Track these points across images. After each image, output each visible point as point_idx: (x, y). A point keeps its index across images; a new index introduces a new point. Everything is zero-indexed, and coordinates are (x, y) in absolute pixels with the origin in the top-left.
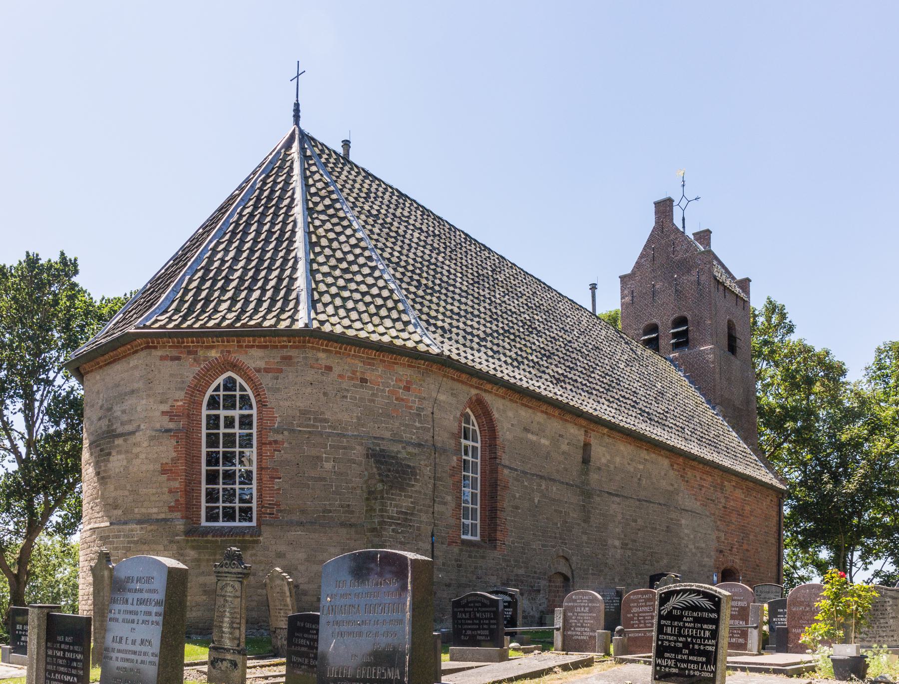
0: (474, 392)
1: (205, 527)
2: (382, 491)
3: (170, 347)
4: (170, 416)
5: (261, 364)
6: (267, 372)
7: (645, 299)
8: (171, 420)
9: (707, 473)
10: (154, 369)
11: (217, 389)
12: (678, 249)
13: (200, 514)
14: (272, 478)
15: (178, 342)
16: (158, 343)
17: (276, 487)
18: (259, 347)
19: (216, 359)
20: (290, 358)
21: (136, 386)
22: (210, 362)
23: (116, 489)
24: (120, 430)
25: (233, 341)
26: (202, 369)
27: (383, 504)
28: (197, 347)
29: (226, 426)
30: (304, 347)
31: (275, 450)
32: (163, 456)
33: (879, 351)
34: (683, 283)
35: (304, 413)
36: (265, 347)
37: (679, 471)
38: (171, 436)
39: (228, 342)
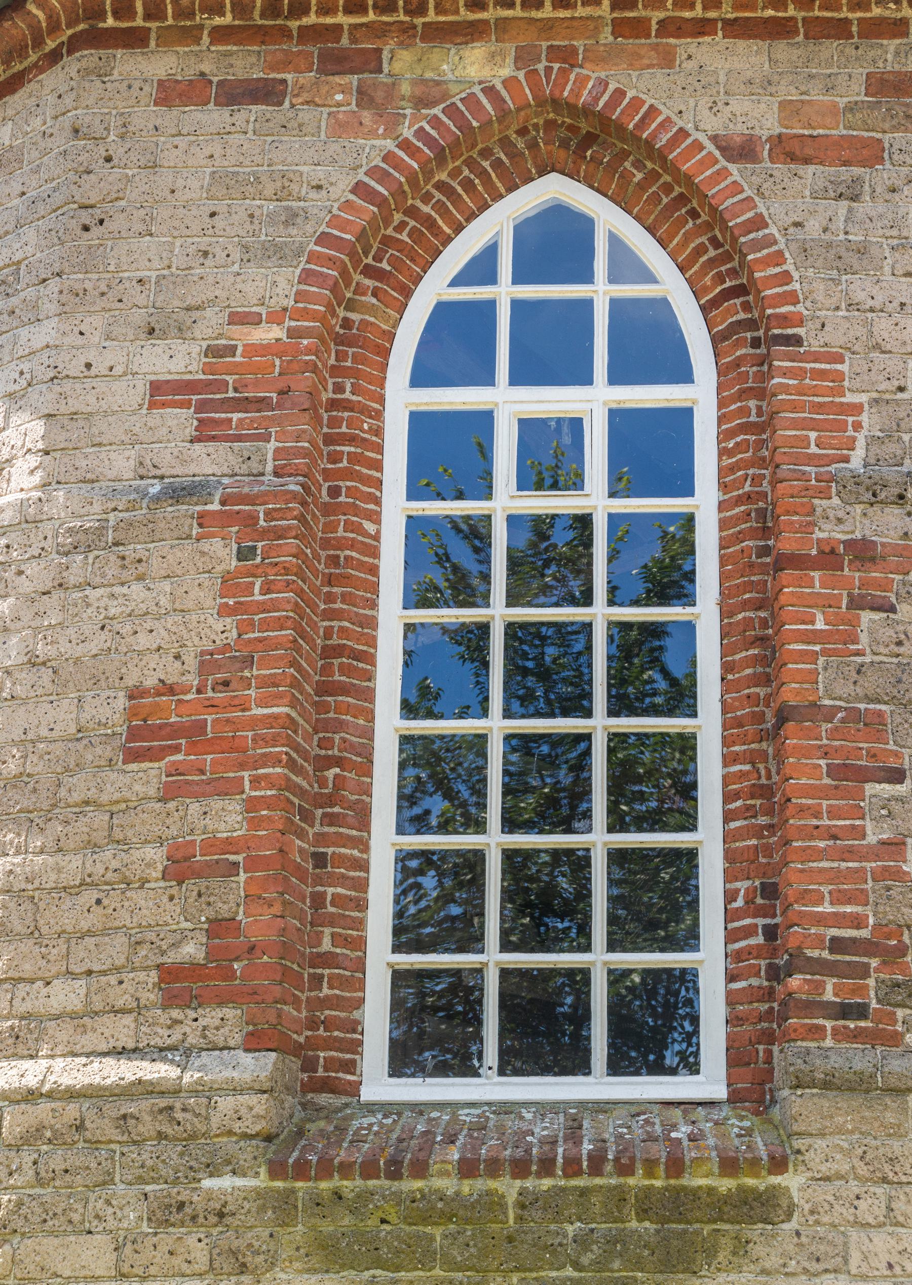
6: (792, 157)
10: (118, 152)
13: (355, 1026)
19: (490, 91)
22: (451, 111)
26: (405, 145)
28: (379, 31)
32: (143, 641)
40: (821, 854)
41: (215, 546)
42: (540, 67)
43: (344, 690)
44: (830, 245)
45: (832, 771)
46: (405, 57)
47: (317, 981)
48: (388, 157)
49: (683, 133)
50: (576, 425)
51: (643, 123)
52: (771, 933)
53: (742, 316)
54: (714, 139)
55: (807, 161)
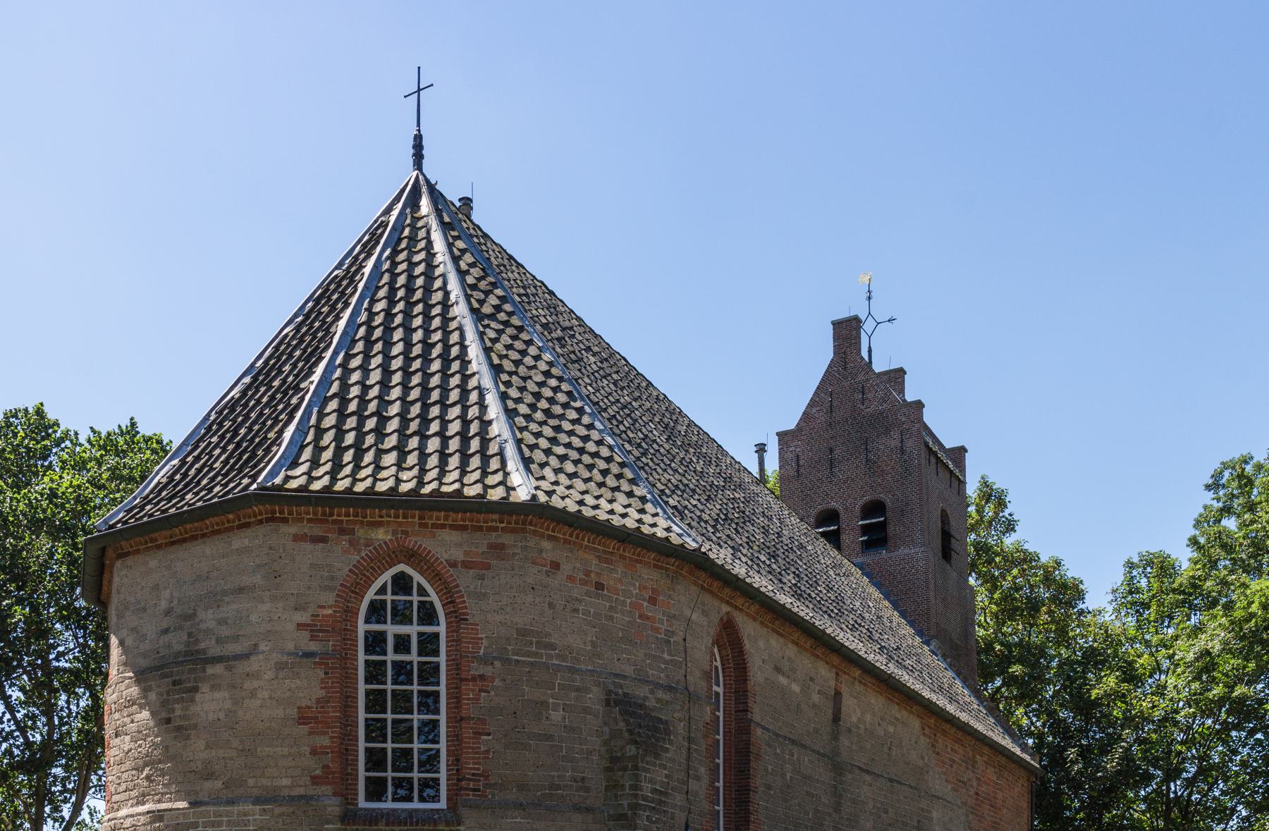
0: (725, 608)
1: (366, 809)
2: (635, 758)
3: (309, 521)
4: (311, 631)
5: (458, 555)
6: (466, 567)
7: (819, 471)
8: (313, 638)
9: (957, 741)
11: (382, 590)
12: (870, 396)
13: (356, 790)
14: (478, 734)
15: (324, 514)
16: (290, 513)
17: (483, 749)
18: (453, 527)
19: (385, 543)
20: (502, 547)
21: (247, 580)
23: (208, 747)
24: (215, 651)
25: (413, 517)
26: (362, 558)
27: (637, 778)
28: (355, 523)
29: (397, 650)
30: (524, 531)
31: (481, 691)
32: (301, 695)
33: (1130, 565)
34: (878, 449)
35: (523, 633)
36: (463, 528)
37: (930, 738)
38: (315, 663)
39: (405, 517)
40: (469, 753)
41: (318, 671)
42: (399, 536)
43: (351, 707)
44: (476, 593)
45: (474, 733)
46: (362, 531)
47: (347, 779)
48: (358, 562)
49: (438, 559)
50: (409, 636)
51: (427, 555)
52: (458, 770)
53: (453, 609)
54: (446, 561)
55: (471, 568)
